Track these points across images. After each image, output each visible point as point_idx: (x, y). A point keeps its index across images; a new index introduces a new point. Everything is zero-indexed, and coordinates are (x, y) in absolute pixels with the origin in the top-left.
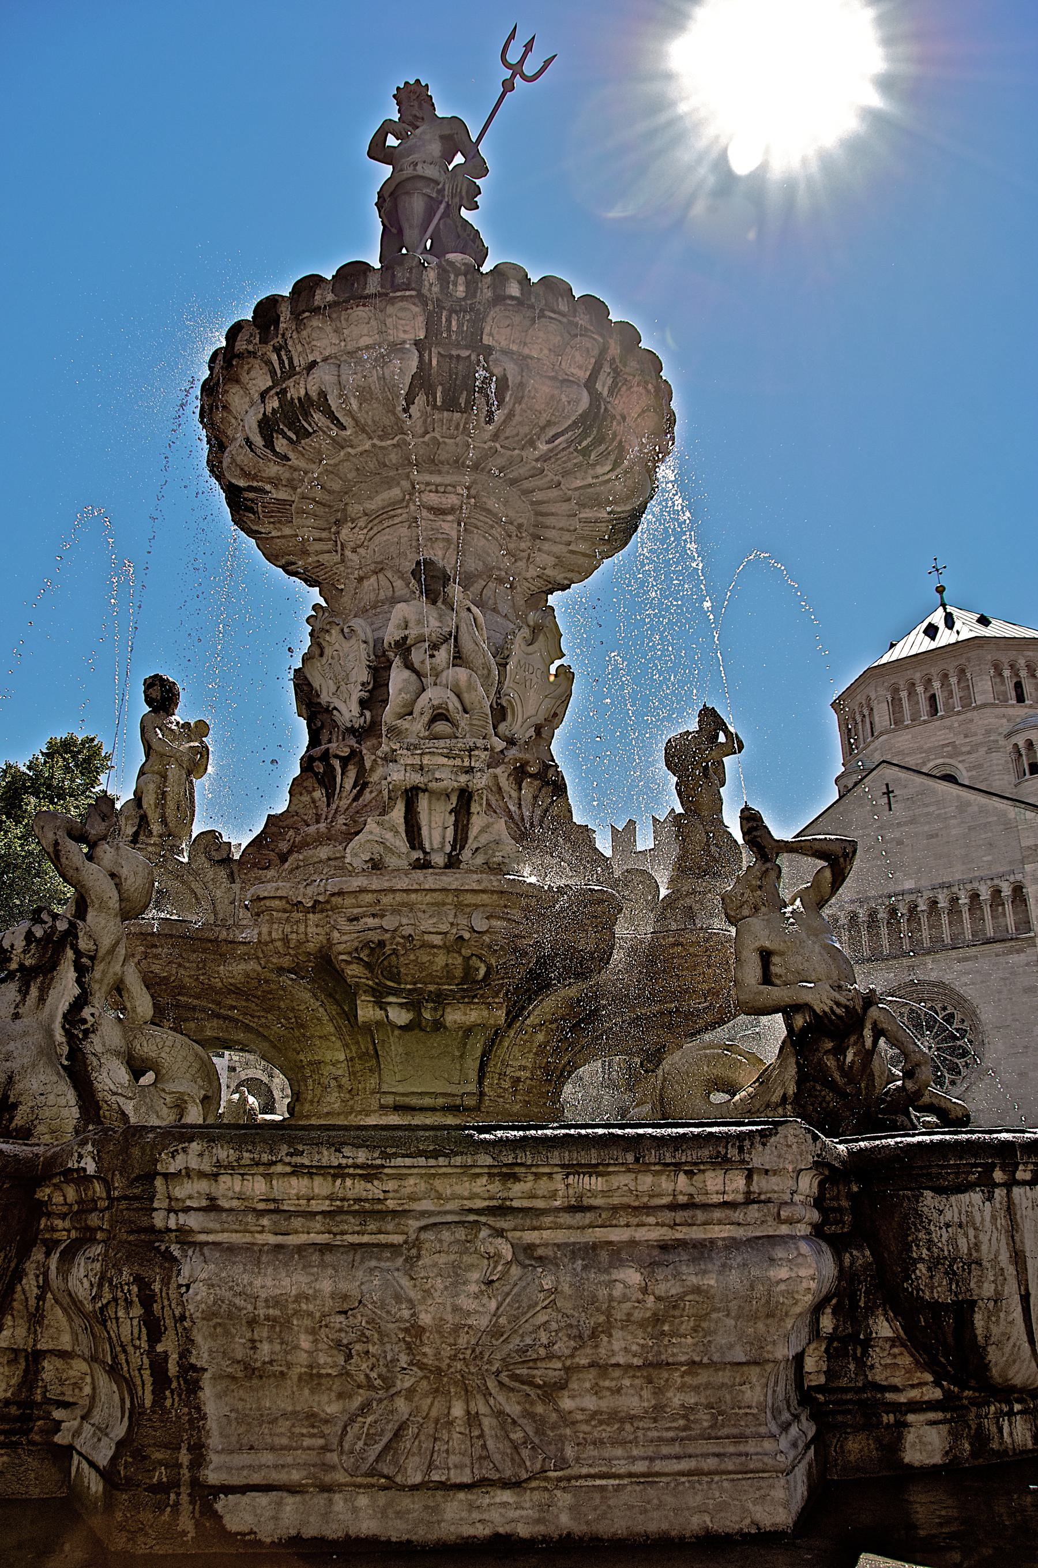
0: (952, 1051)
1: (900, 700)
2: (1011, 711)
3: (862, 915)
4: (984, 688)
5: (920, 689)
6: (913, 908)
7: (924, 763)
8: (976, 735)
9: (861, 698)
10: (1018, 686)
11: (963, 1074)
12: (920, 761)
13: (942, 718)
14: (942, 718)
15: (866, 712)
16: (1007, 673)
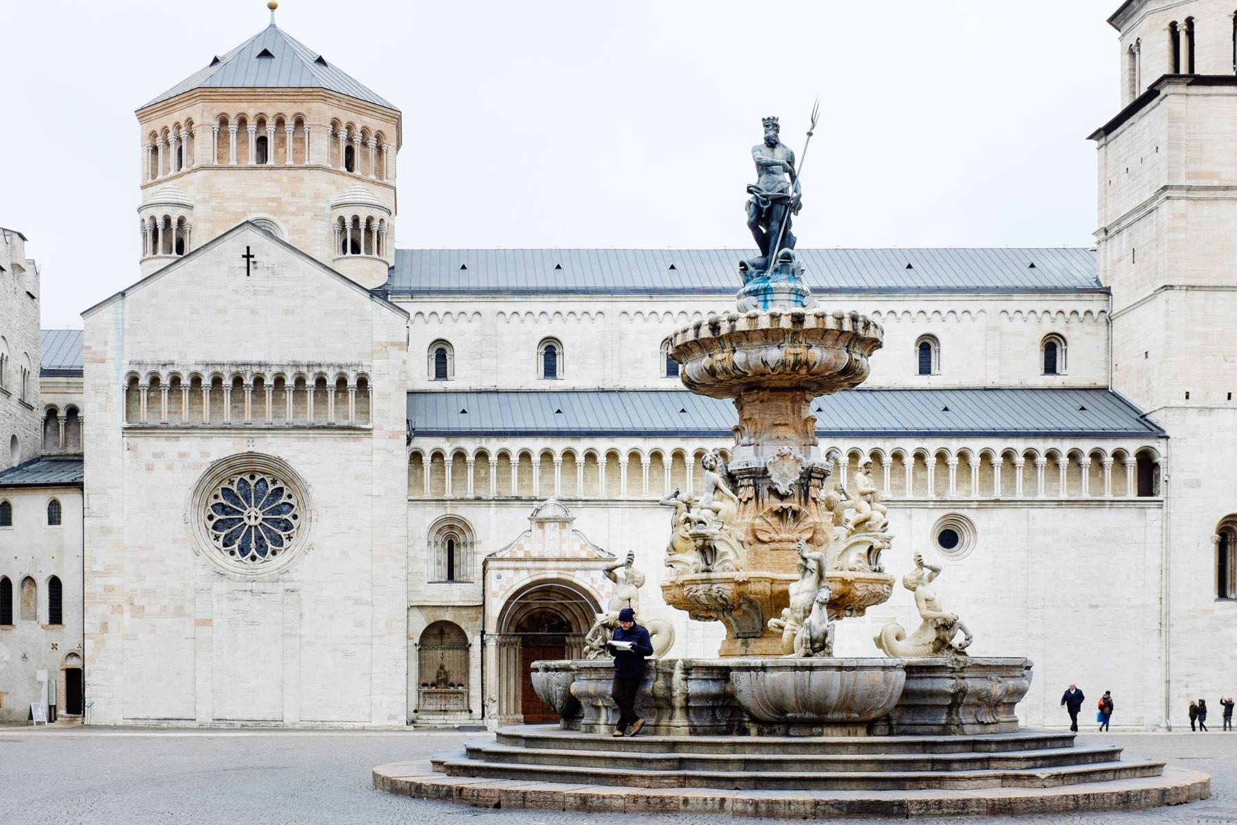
0: (277, 523)
1: (227, 134)
2: (340, 178)
3: (206, 381)
4: (320, 148)
5: (252, 126)
6: (259, 380)
7: (244, 213)
8: (304, 196)
9: (180, 116)
10: (350, 151)
11: (285, 546)
12: (241, 210)
13: (271, 168)
14: (271, 168)
15: (183, 134)
16: (343, 134)
